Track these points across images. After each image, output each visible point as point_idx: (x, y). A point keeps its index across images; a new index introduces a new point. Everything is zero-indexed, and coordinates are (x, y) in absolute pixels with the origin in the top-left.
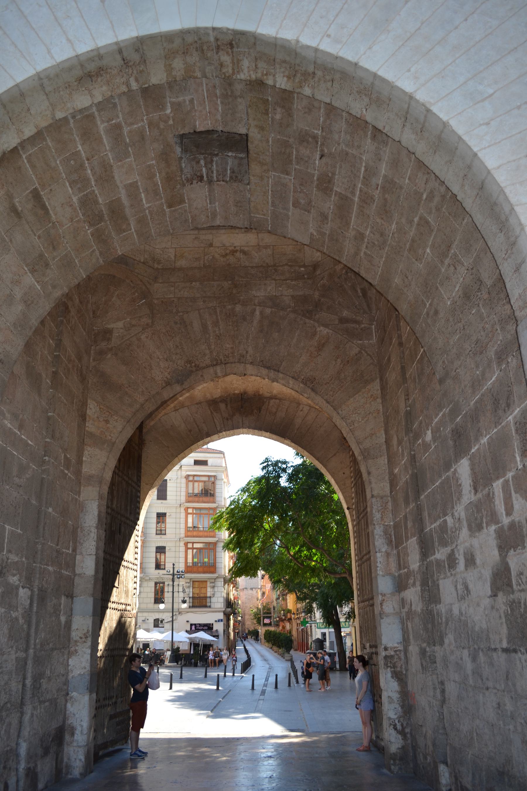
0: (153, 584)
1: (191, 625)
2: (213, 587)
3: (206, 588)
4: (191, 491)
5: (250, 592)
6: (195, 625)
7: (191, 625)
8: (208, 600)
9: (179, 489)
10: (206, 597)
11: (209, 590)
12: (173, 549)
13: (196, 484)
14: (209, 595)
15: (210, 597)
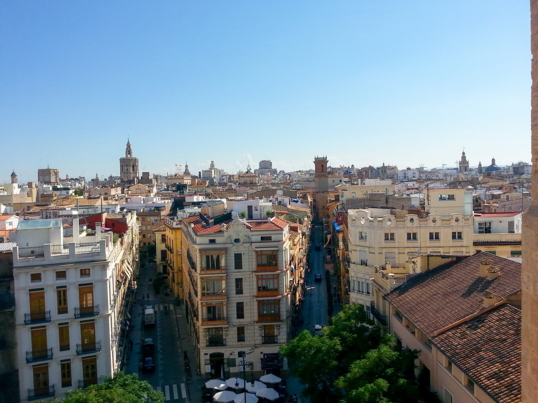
0: (236, 329)
1: (264, 355)
2: (279, 329)
3: (274, 329)
4: (260, 263)
5: (322, 194)
6: (267, 354)
7: (264, 355)
8: (275, 338)
9: (250, 260)
10: (274, 336)
11: (276, 330)
12: (249, 304)
13: (263, 256)
14: (275, 334)
15: (277, 336)
